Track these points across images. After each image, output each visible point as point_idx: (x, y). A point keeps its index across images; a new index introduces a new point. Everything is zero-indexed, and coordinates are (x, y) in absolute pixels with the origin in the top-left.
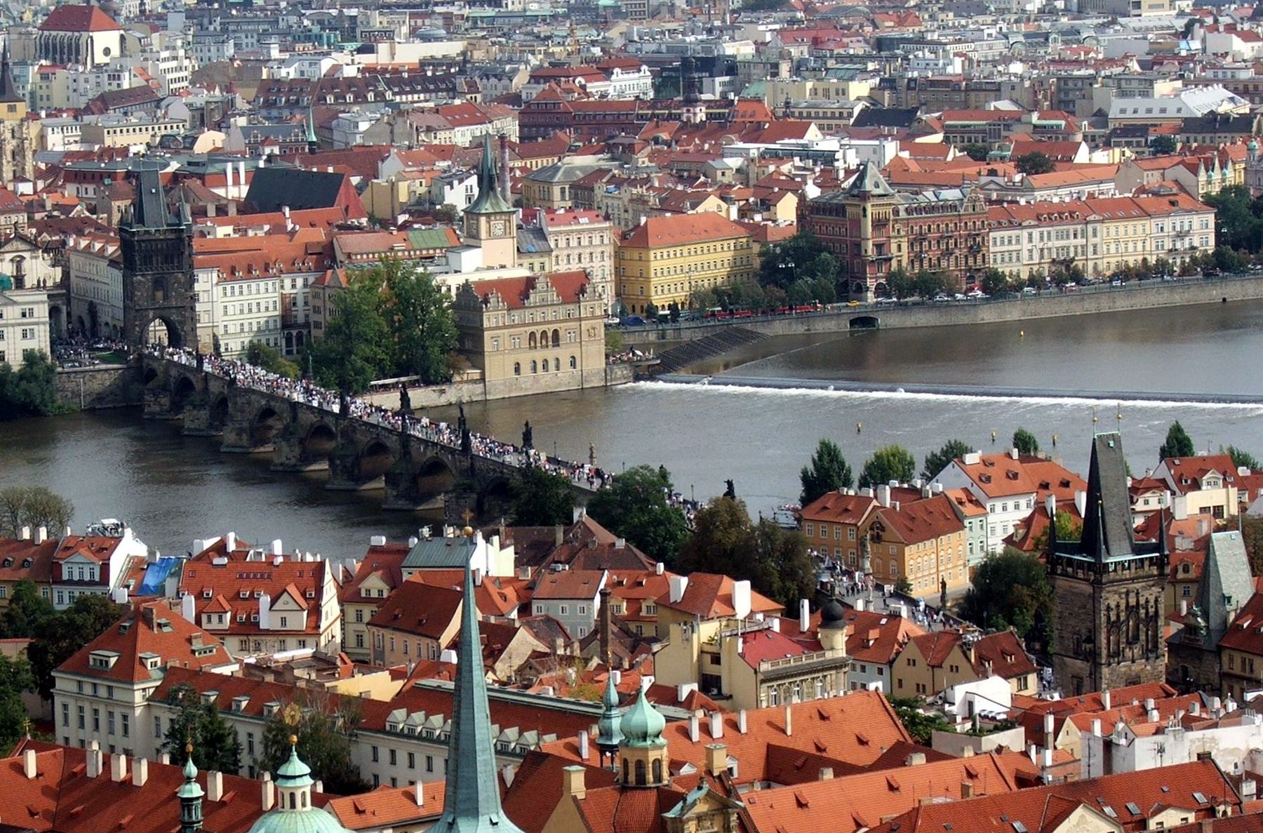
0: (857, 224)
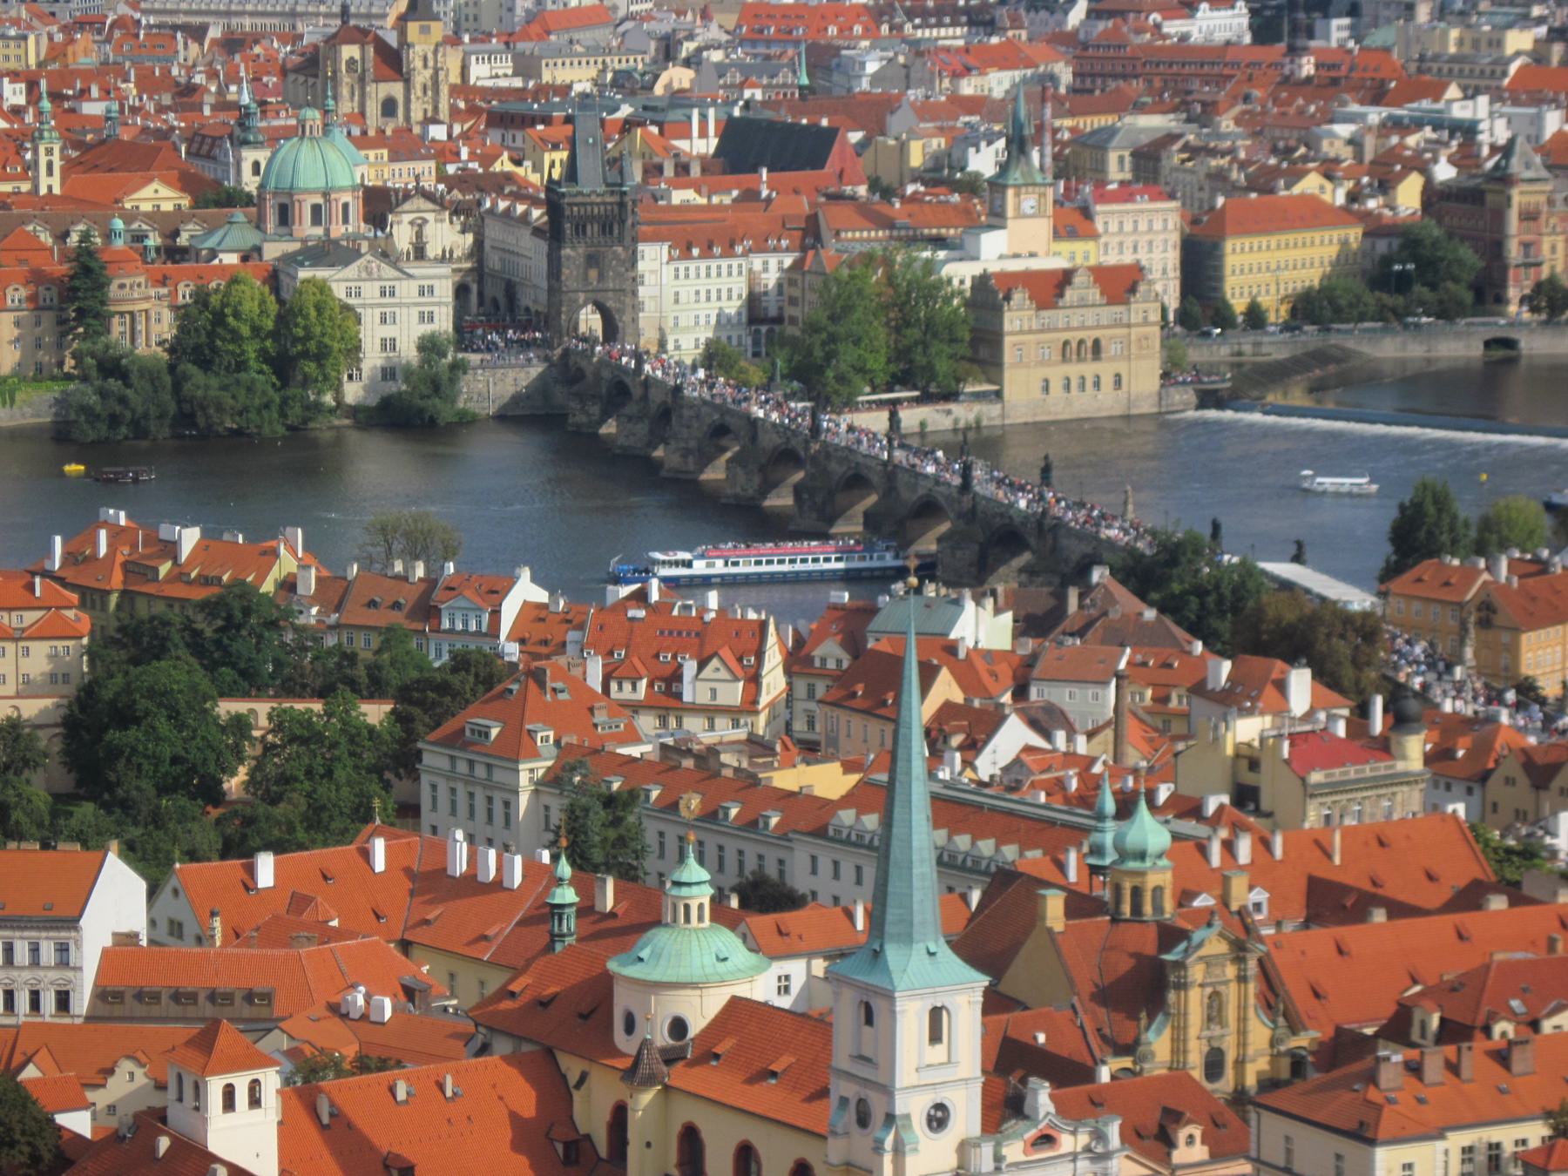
0: (1499, 216)
